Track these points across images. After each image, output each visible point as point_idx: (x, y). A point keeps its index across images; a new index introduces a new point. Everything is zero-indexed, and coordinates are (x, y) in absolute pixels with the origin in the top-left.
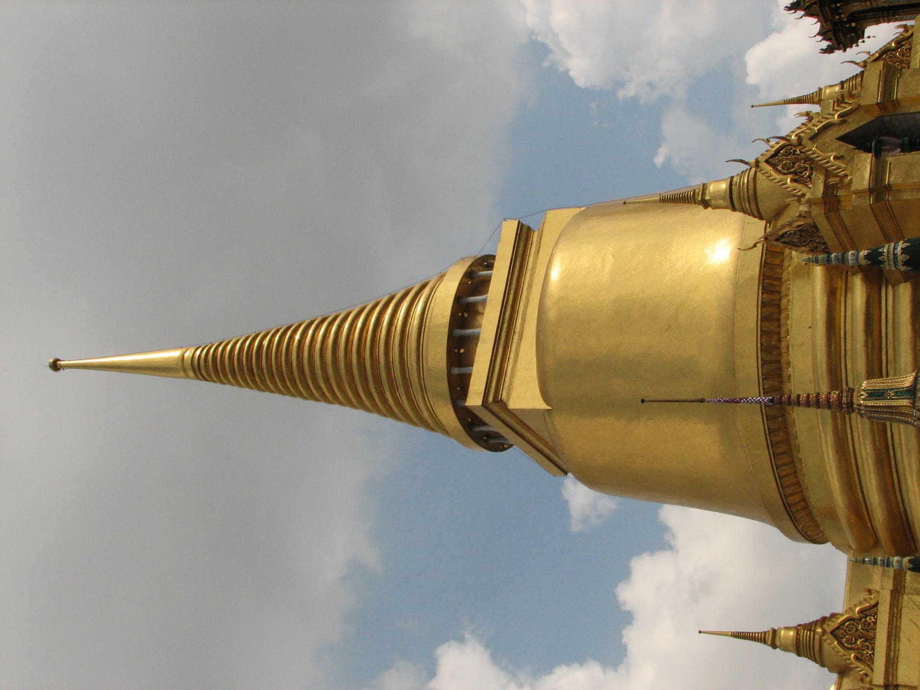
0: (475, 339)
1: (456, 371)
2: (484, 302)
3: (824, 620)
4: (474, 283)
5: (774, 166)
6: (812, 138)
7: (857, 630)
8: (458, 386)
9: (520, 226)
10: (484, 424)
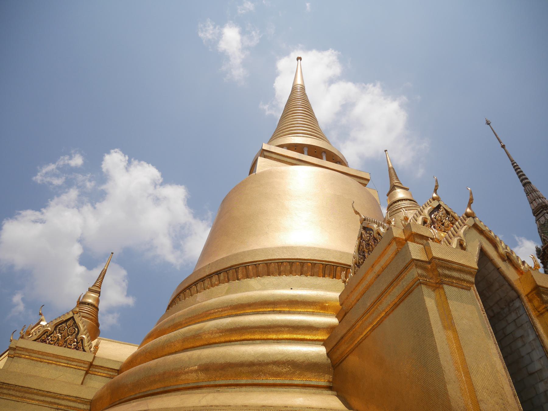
0: (303, 153)
6: (475, 226)
7: (68, 335)
9: (368, 180)
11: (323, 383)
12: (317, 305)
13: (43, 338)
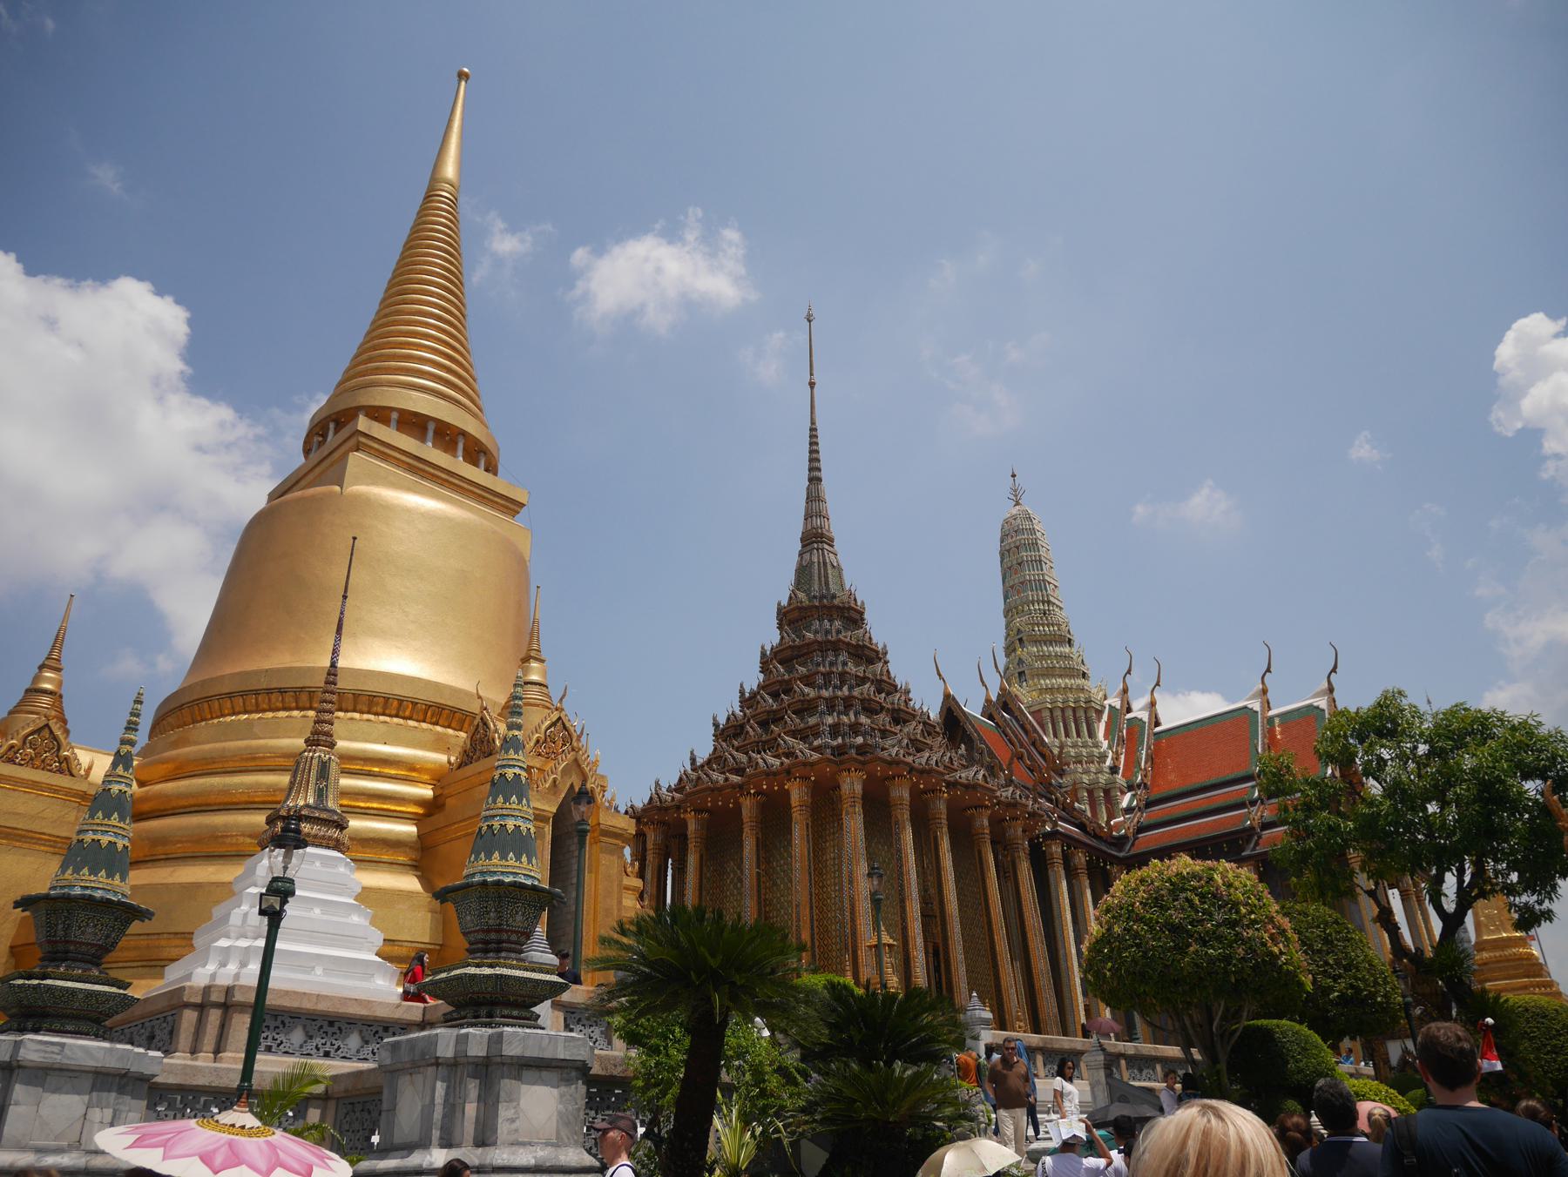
0: (422, 438)
1: (395, 416)
2: (455, 456)
3: (65, 722)
4: (477, 452)
5: (554, 724)
6: (576, 760)
8: (380, 414)
9: (523, 505)
10: (336, 431)
11: (401, 859)
12: (409, 770)
13: (10, 754)
